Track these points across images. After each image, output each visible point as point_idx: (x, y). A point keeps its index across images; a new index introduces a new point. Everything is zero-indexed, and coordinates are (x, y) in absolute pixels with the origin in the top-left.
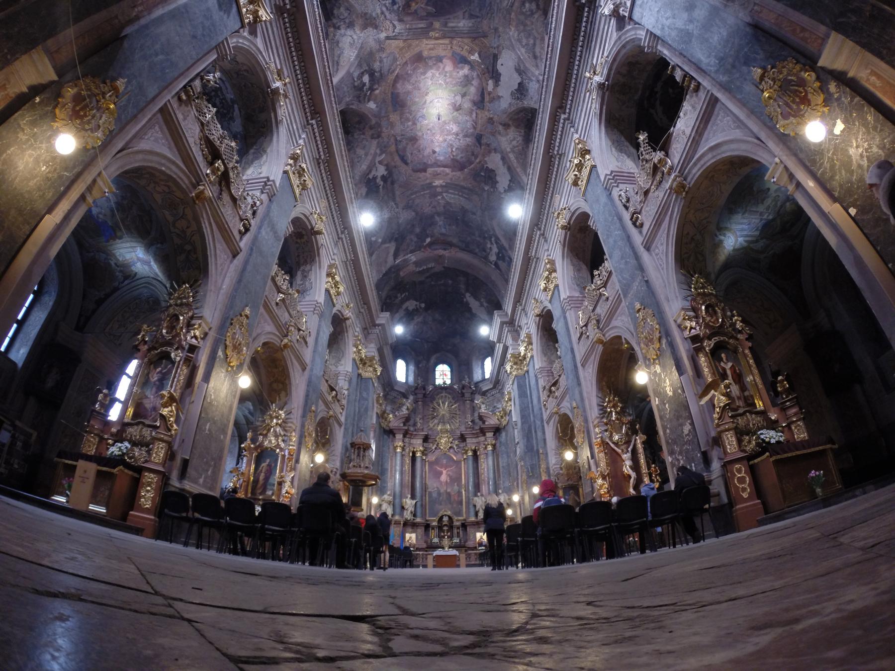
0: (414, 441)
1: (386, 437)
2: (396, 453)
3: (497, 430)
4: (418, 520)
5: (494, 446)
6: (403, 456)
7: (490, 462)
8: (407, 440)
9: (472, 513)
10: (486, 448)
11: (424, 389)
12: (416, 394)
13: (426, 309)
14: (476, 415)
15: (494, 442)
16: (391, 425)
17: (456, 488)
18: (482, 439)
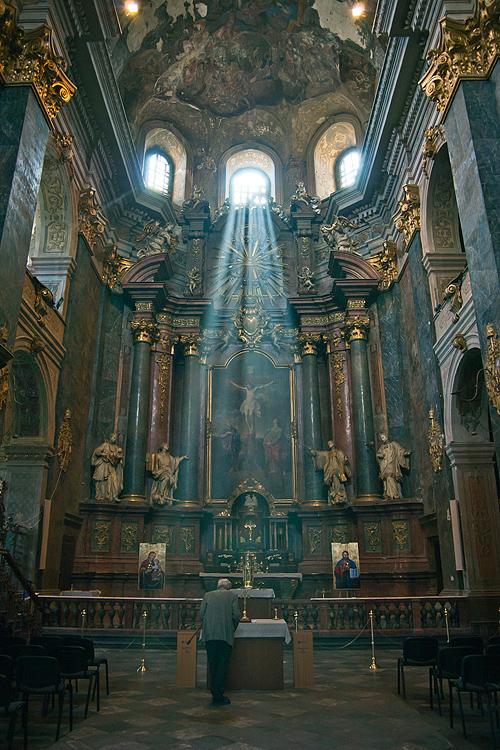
0: (180, 322)
1: (113, 308)
2: (136, 343)
3: (374, 295)
4: (187, 504)
5: (366, 330)
6: (151, 353)
7: (359, 369)
8: (163, 318)
9: (315, 491)
10: (346, 338)
11: (207, 210)
12: (188, 222)
13: (212, 23)
14: (323, 269)
15: (367, 321)
16: (125, 280)
17: (275, 429)
18: (339, 316)
